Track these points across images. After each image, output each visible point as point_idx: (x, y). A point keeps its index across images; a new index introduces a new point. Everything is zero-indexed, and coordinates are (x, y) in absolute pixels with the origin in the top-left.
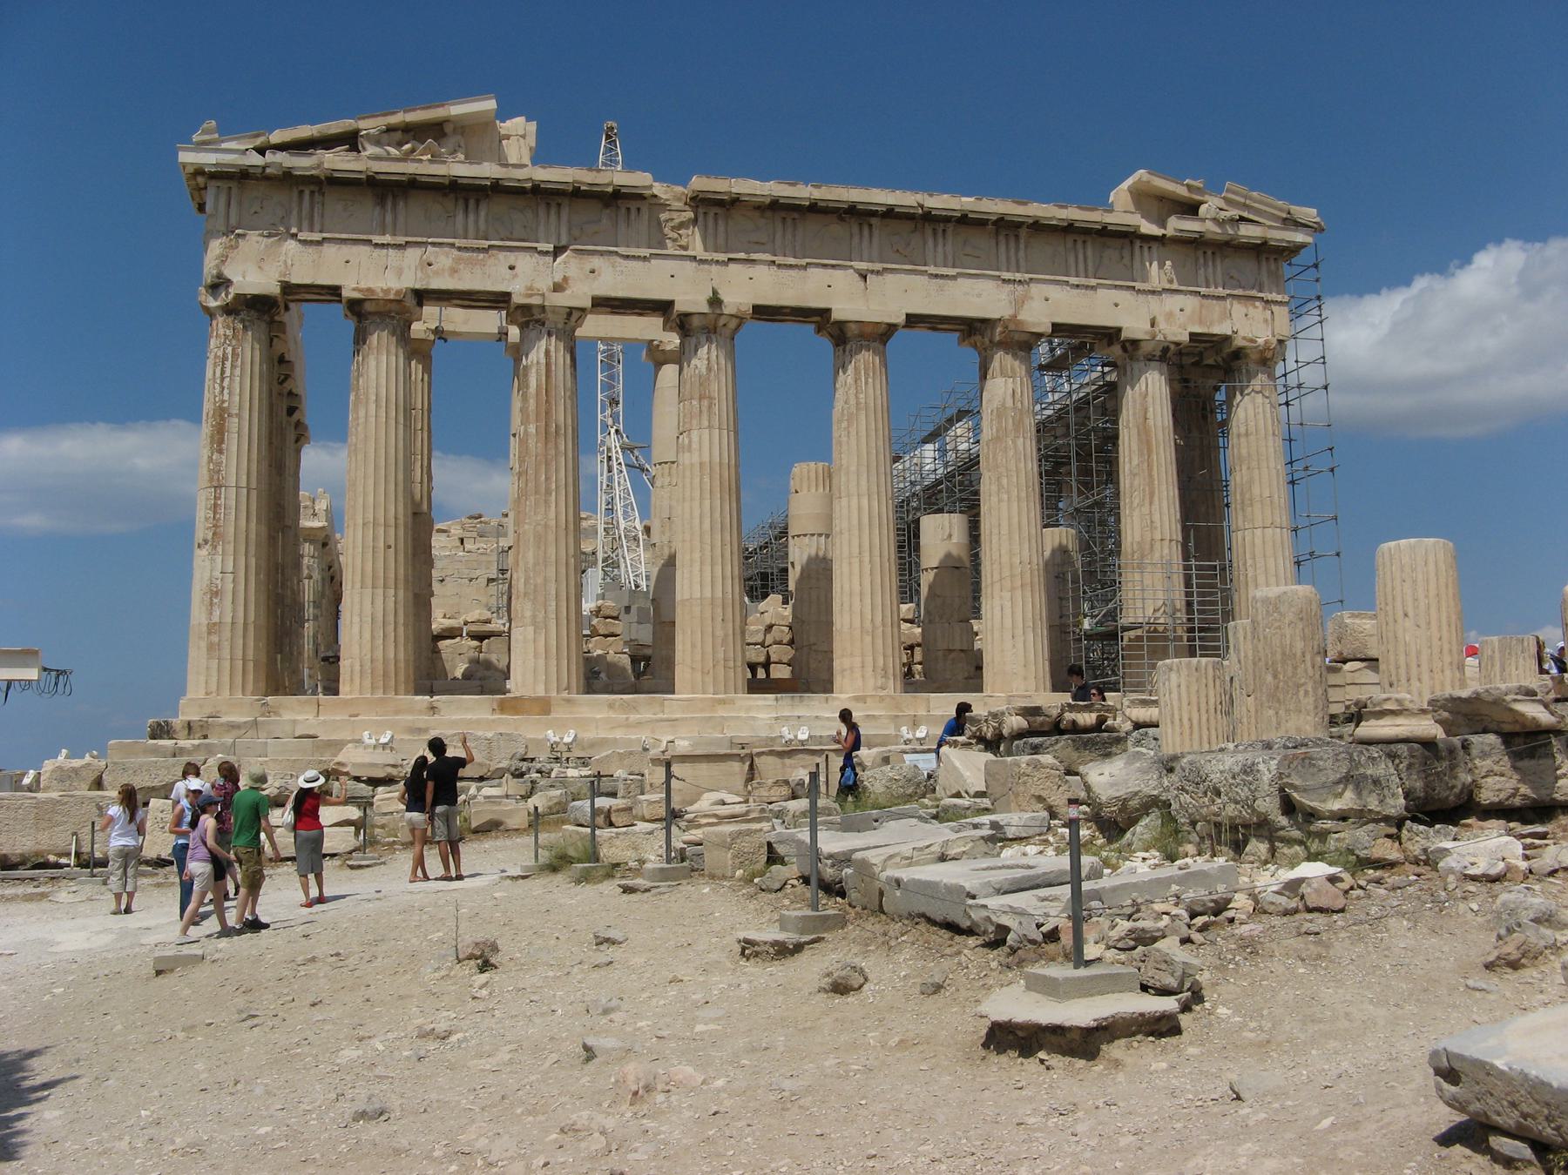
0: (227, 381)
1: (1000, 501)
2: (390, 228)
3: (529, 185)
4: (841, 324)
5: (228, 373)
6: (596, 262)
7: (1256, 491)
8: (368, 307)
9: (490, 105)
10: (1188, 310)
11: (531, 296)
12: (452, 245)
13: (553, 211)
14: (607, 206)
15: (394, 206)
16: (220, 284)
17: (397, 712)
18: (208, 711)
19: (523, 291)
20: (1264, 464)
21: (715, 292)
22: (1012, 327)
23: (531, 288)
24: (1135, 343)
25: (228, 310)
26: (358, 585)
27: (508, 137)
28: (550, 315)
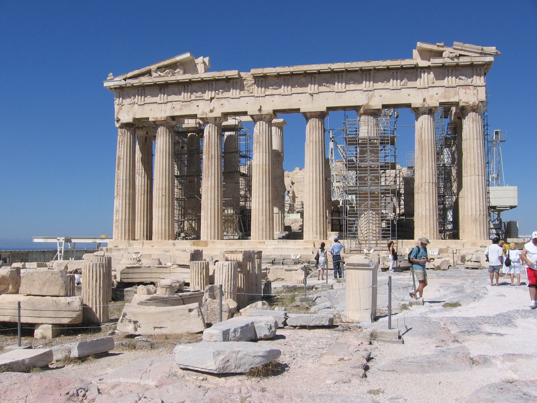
3: (200, 79)
6: (223, 101)
7: (469, 161)
8: (158, 123)
9: (187, 55)
10: (439, 94)
11: (202, 115)
15: (164, 90)
16: (118, 121)
18: (115, 245)
19: (201, 113)
20: (472, 151)
21: (261, 107)
22: (366, 108)
23: (203, 112)
24: (417, 108)
27: (198, 64)
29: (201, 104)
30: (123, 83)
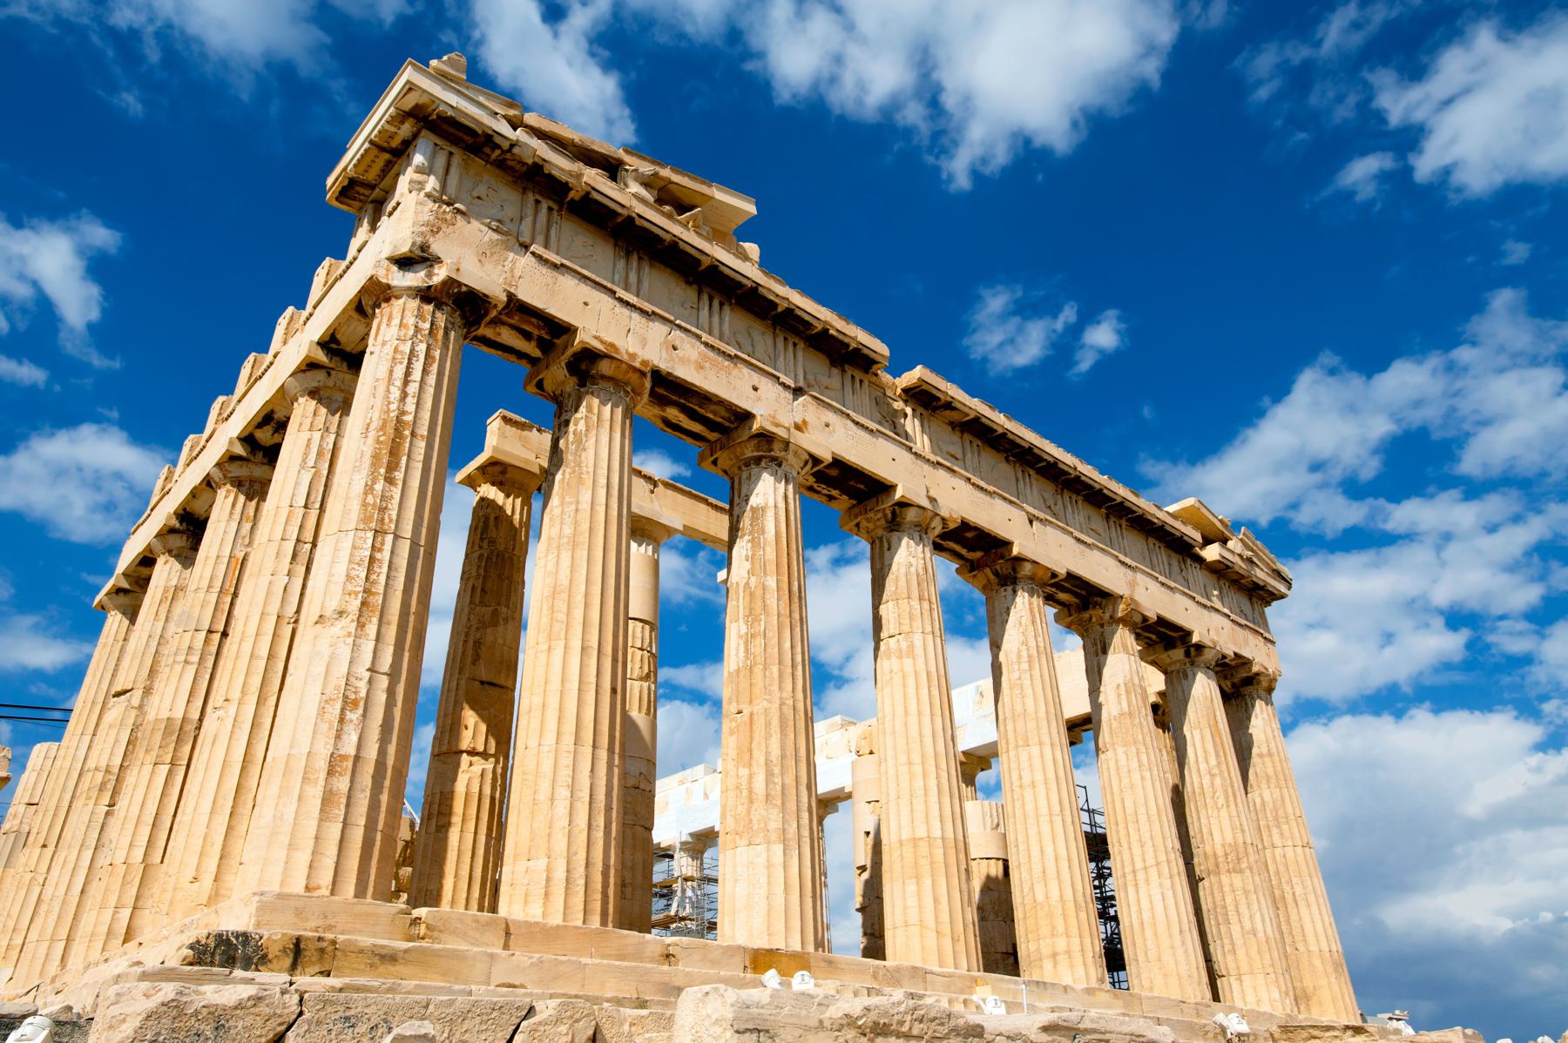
0: (413, 388)
1: (1143, 778)
2: (634, 288)
4: (1020, 560)
5: (417, 374)
6: (830, 417)
9: (749, 207)
11: (777, 425)
12: (699, 337)
13: (791, 347)
14: (833, 363)
17: (621, 957)
24: (1200, 647)
25: (426, 295)
26: (569, 739)
28: (790, 457)
29: (768, 388)
30: (504, 128)
